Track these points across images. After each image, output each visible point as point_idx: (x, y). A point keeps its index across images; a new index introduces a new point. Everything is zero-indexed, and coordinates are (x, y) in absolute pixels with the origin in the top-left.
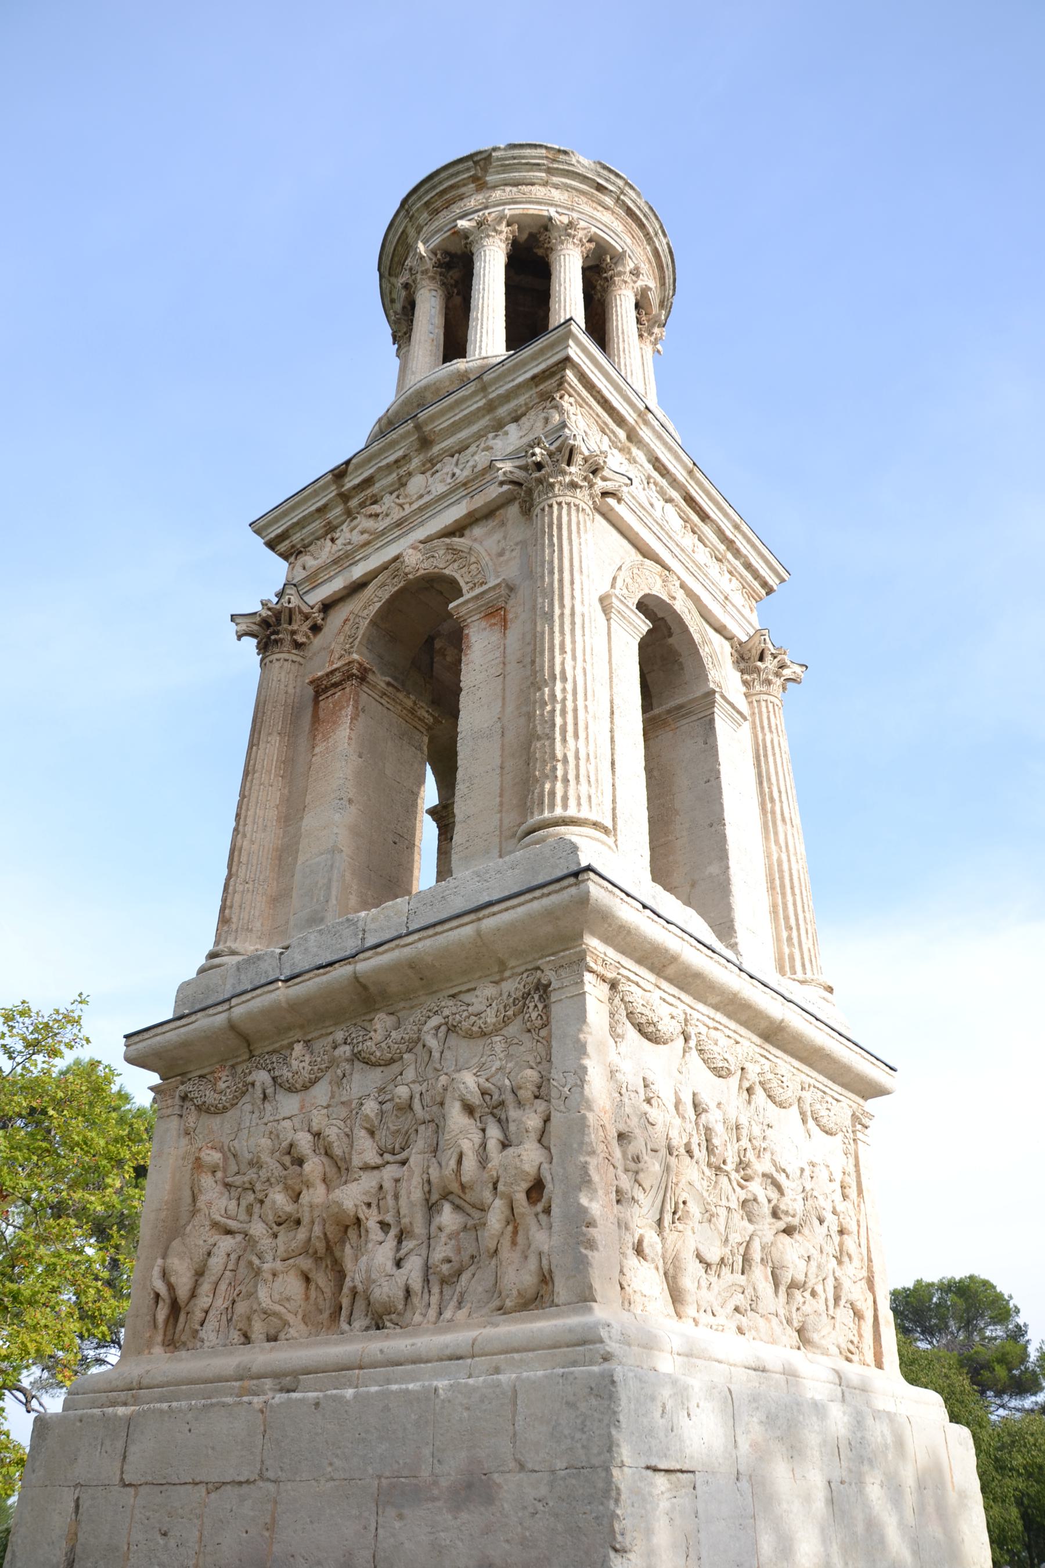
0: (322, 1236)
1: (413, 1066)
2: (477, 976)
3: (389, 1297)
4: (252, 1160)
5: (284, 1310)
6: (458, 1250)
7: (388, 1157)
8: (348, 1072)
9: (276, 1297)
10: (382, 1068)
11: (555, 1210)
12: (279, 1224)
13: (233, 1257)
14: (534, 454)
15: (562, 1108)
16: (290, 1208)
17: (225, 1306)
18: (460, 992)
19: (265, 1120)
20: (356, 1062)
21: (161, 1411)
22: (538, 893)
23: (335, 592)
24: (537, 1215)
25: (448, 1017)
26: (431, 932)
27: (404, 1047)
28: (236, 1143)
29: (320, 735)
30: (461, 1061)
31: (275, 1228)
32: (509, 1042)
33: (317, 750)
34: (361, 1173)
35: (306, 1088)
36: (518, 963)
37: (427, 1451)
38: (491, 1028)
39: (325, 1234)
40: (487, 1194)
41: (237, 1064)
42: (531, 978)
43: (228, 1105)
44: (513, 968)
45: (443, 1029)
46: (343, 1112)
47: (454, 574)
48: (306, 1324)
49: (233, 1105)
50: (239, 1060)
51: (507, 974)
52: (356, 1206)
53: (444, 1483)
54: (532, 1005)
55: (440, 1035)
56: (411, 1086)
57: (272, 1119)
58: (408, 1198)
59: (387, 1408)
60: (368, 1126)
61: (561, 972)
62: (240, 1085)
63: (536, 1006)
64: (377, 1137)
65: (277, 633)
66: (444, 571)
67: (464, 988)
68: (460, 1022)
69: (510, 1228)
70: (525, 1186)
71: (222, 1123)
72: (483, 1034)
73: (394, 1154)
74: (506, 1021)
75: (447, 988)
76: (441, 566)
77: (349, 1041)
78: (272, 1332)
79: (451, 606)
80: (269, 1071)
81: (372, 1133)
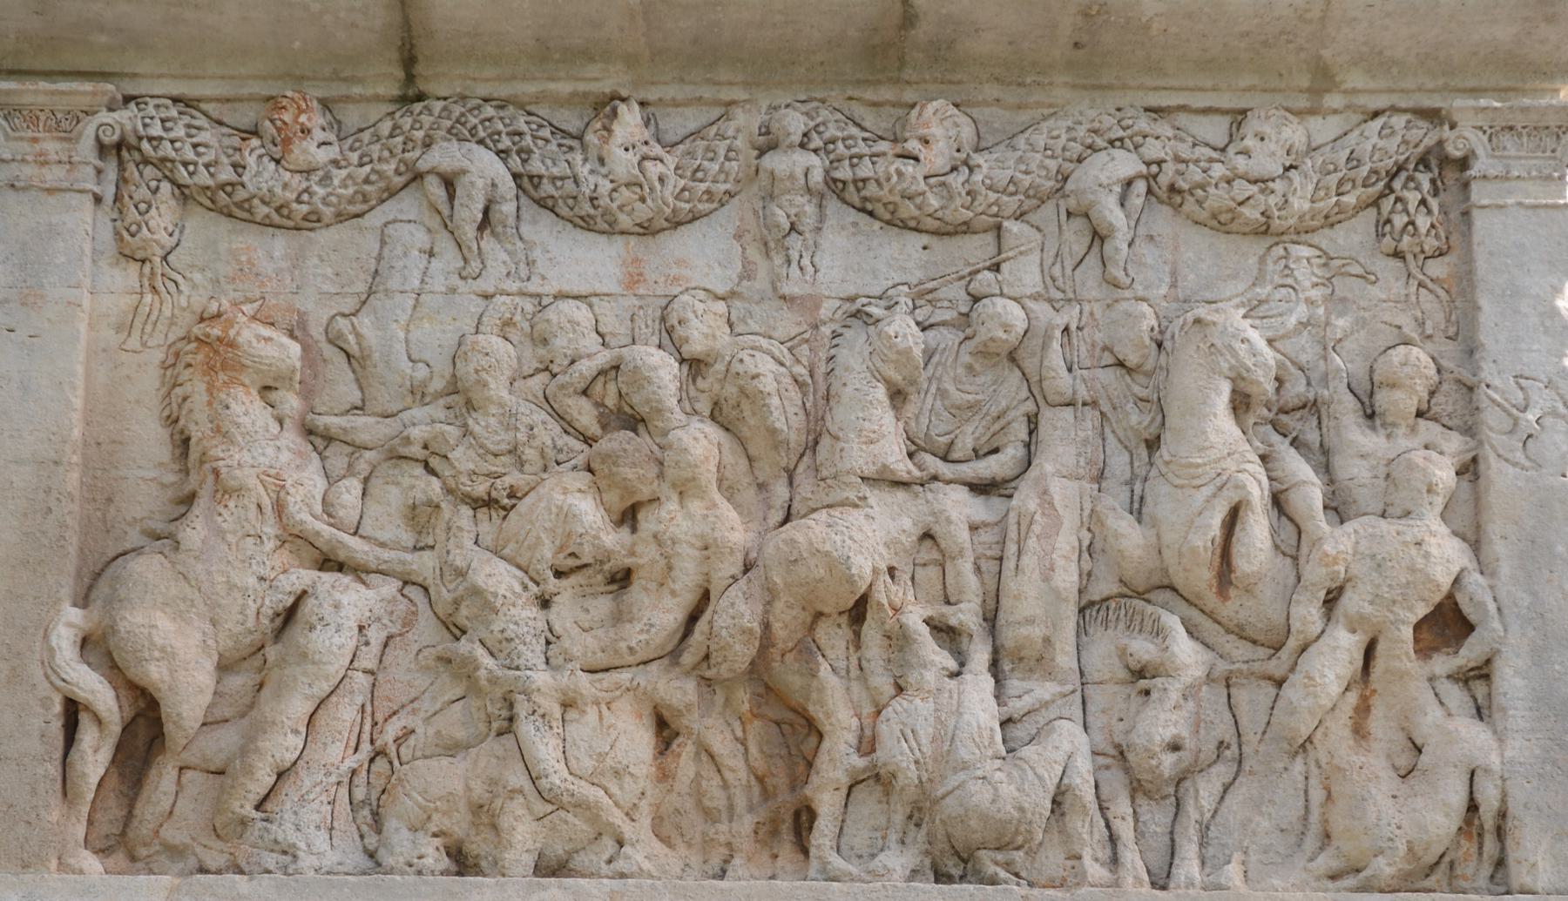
0: (756, 627)
1: (1035, 257)
2: (1243, 84)
3: (1021, 810)
4: (424, 384)
5: (606, 800)
6: (1197, 725)
7: (934, 464)
8: (808, 222)
9: (588, 764)
10: (925, 239)
11: (1511, 680)
12: (559, 574)
13: (376, 635)
15: (1519, 456)
16: (613, 539)
17: (351, 762)
18: (1183, 108)
19: (486, 285)
20: (832, 205)
24: (1431, 679)
25: (1160, 163)
27: (1011, 204)
28: (365, 323)
30: (1190, 280)
31: (552, 584)
32: (1332, 267)
34: (866, 490)
35: (647, 230)
36: (1372, 85)
38: (1291, 222)
39: (767, 626)
40: (1308, 613)
41: (347, 99)
42: (1415, 134)
43: (328, 212)
44: (1355, 91)
45: (1140, 187)
46: (788, 323)
48: (666, 841)
49: (341, 217)
50: (356, 90)
51: (1334, 100)
52: (875, 571)
54: (1413, 198)
56: (1030, 304)
57: (514, 286)
58: (1046, 579)
60: (897, 377)
61: (1506, 139)
62: (389, 168)
63: (1423, 202)
64: (910, 409)
67: (1200, 101)
69: (1353, 698)
70: (1422, 610)
71: (297, 261)
72: (1264, 230)
73: (945, 459)
74: (1329, 222)
75: (1140, 87)
77: (817, 142)
78: (559, 849)
80: (503, 154)
81: (897, 396)
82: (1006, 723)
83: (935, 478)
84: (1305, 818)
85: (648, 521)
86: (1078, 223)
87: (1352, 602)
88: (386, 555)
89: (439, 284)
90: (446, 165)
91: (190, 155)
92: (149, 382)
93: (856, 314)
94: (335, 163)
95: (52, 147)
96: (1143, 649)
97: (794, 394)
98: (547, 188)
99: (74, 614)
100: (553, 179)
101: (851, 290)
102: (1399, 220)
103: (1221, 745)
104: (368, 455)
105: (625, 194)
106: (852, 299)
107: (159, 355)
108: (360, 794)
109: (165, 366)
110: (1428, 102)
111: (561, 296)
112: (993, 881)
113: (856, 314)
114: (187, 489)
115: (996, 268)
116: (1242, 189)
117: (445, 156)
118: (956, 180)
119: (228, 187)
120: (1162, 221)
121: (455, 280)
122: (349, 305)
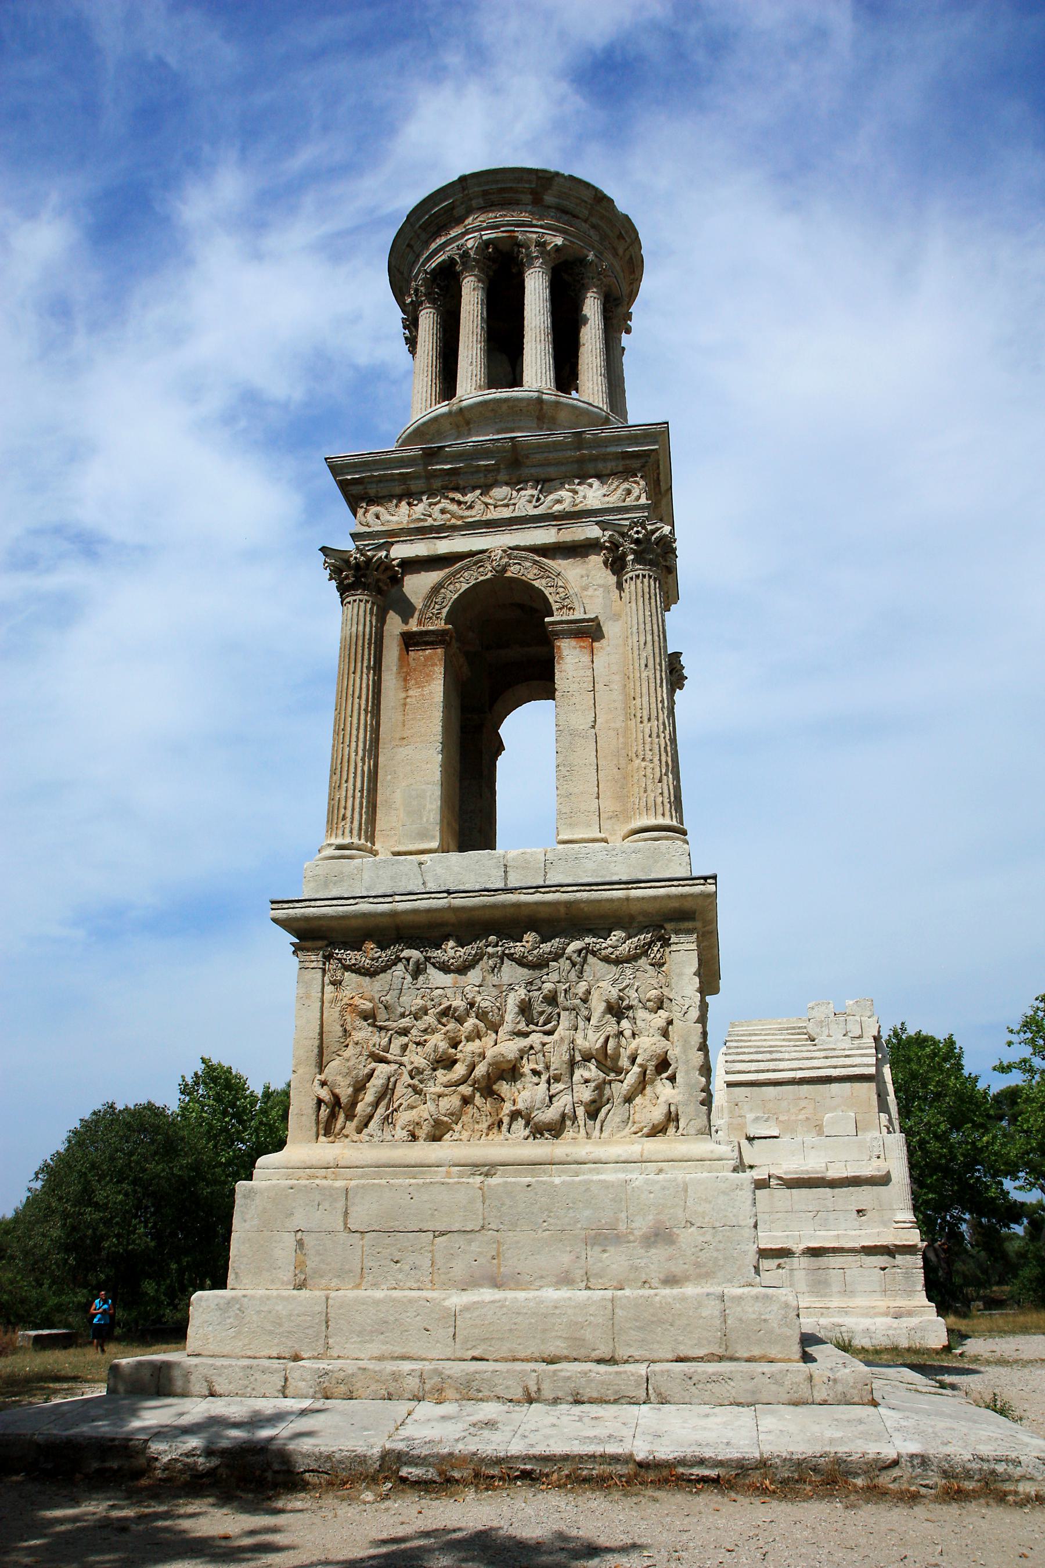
4: (404, 1012)
13: (392, 1079)
14: (638, 532)
17: (388, 1112)
18: (596, 929)
21: (380, 1185)
22: (675, 883)
23: (417, 556)
25: (589, 944)
26: (587, 888)
28: (388, 997)
29: (413, 681)
30: (598, 975)
31: (436, 1065)
33: (411, 693)
37: (623, 1215)
46: (495, 992)
47: (543, 589)
53: (637, 1233)
55: (582, 955)
57: (424, 986)
59: (587, 1190)
63: (658, 950)
65: (364, 576)
66: (534, 583)
67: (600, 927)
68: (600, 949)
72: (617, 962)
76: (529, 576)
79: (547, 619)
80: (422, 952)
82: (551, 1097)
83: (534, 1031)
84: (629, 1118)
85: (460, 1048)
86: (568, 961)
87: (639, 1061)
88: (396, 1058)
89: (405, 986)
90: (407, 956)
91: (345, 957)
92: (337, 1015)
93: (512, 989)
94: (380, 957)
95: (313, 958)
96: (587, 1075)
97: (497, 1011)
98: (433, 960)
99: (319, 1077)
100: (434, 958)
101: (510, 982)
102: (652, 955)
103: (609, 1100)
104: (391, 1032)
105: (452, 961)
106: (511, 985)
107: (339, 1008)
108: (390, 1121)
109: (340, 1011)
110: (659, 923)
111: (436, 988)
112: (547, 1139)
113: (512, 989)
114: (347, 1043)
115: (548, 974)
116: (610, 950)
117: (406, 953)
118: (535, 952)
119: (354, 965)
120: (590, 958)
121: (410, 985)
122: (384, 993)
